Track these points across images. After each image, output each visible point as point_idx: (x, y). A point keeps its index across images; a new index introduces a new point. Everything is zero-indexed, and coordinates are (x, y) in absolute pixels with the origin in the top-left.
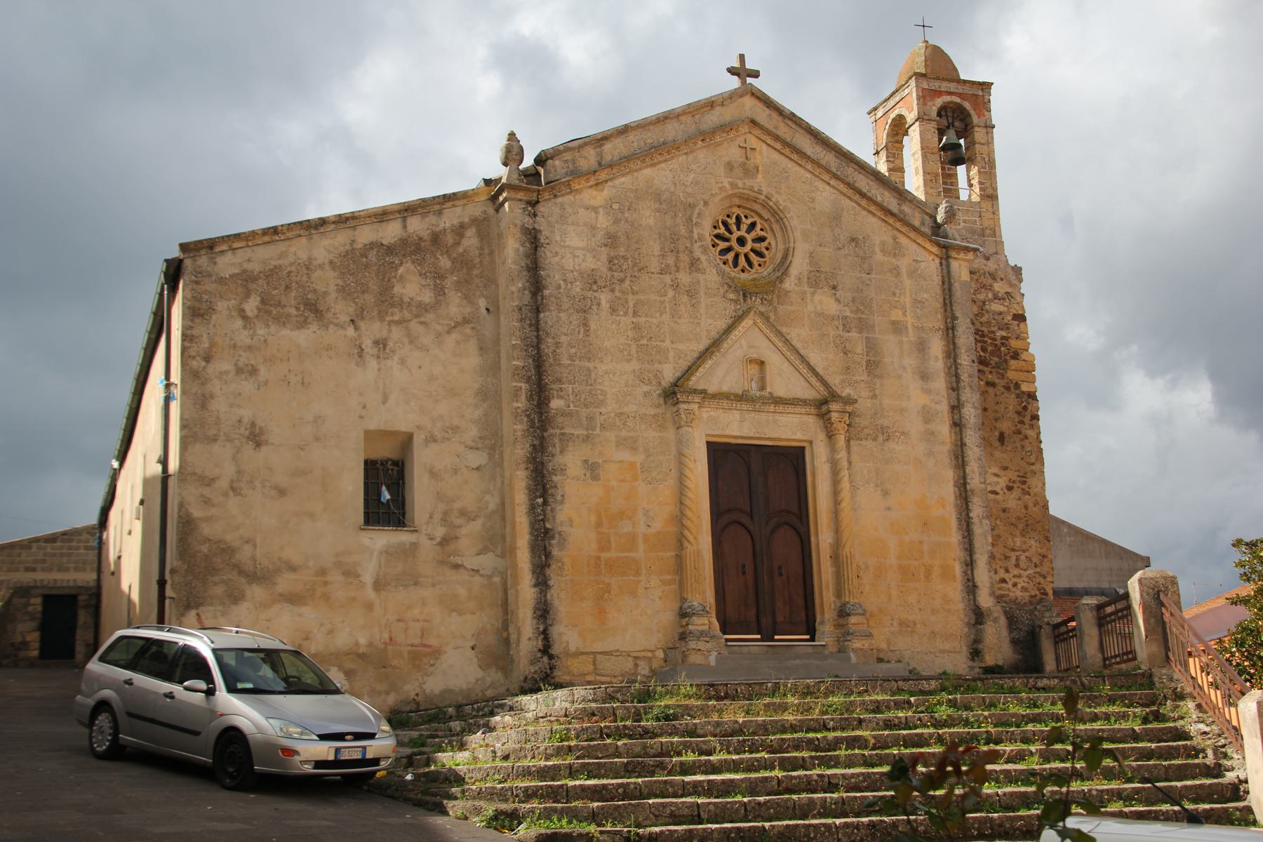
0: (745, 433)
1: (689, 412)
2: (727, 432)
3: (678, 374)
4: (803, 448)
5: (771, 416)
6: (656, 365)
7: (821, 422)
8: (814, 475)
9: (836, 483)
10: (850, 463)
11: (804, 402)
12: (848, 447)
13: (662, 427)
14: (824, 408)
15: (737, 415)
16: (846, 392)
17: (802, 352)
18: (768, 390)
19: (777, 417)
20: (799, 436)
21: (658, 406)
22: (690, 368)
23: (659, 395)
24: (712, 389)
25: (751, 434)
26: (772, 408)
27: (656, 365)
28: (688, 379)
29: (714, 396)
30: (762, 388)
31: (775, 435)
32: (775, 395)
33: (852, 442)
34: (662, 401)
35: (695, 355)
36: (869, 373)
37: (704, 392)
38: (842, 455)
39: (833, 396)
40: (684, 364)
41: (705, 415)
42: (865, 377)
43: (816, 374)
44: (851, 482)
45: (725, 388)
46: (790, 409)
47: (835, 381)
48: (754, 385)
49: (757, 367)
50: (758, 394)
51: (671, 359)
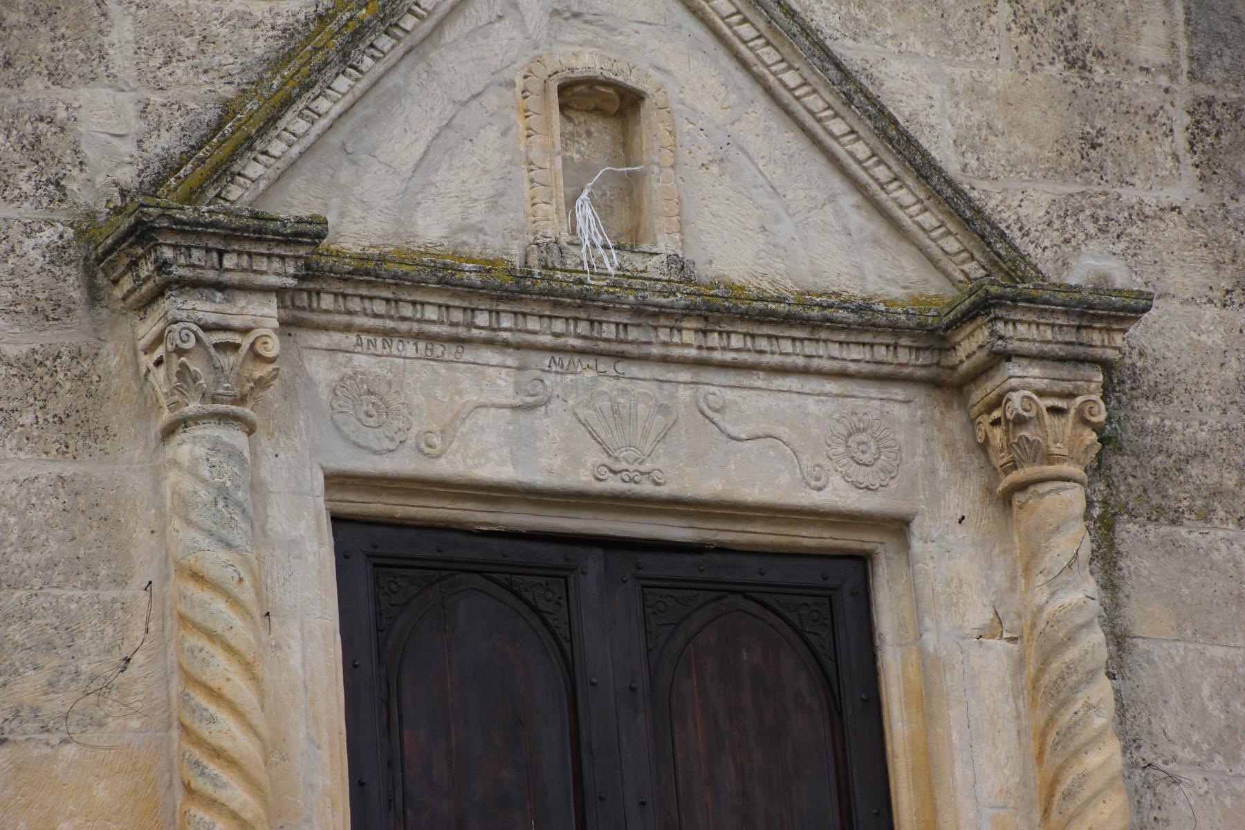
0: (547, 468)
1: (224, 339)
2: (447, 467)
3: (166, 142)
4: (862, 562)
5: (683, 390)
6: (36, 87)
7: (954, 421)
8: (926, 702)
9: (1049, 747)
10: (1119, 639)
11: (859, 320)
12: (1106, 557)
13: (80, 428)
14: (970, 345)
15: (491, 378)
16: (1092, 265)
17: (848, 50)
18: (665, 244)
19: (718, 388)
20: (838, 494)
21: (50, 312)
22: (228, 110)
23: (57, 254)
24: (356, 231)
25: (582, 478)
26: (687, 341)
27: (36, 87)
28: (223, 171)
29: (367, 273)
30: (630, 240)
31: (709, 486)
32: (704, 273)
33: (1127, 531)
34: (74, 291)
35: (261, 46)
36: (1208, 170)
37: (309, 233)
38: (1082, 593)
39: (1002, 286)
40: (197, 93)
41: (320, 370)
42: (1183, 189)
43: (924, 169)
44: (1130, 744)
45: (432, 229)
46: (787, 350)
47: (1024, 204)
48: (585, 212)
49: (602, 131)
50: (611, 262)
51: (121, 59)
